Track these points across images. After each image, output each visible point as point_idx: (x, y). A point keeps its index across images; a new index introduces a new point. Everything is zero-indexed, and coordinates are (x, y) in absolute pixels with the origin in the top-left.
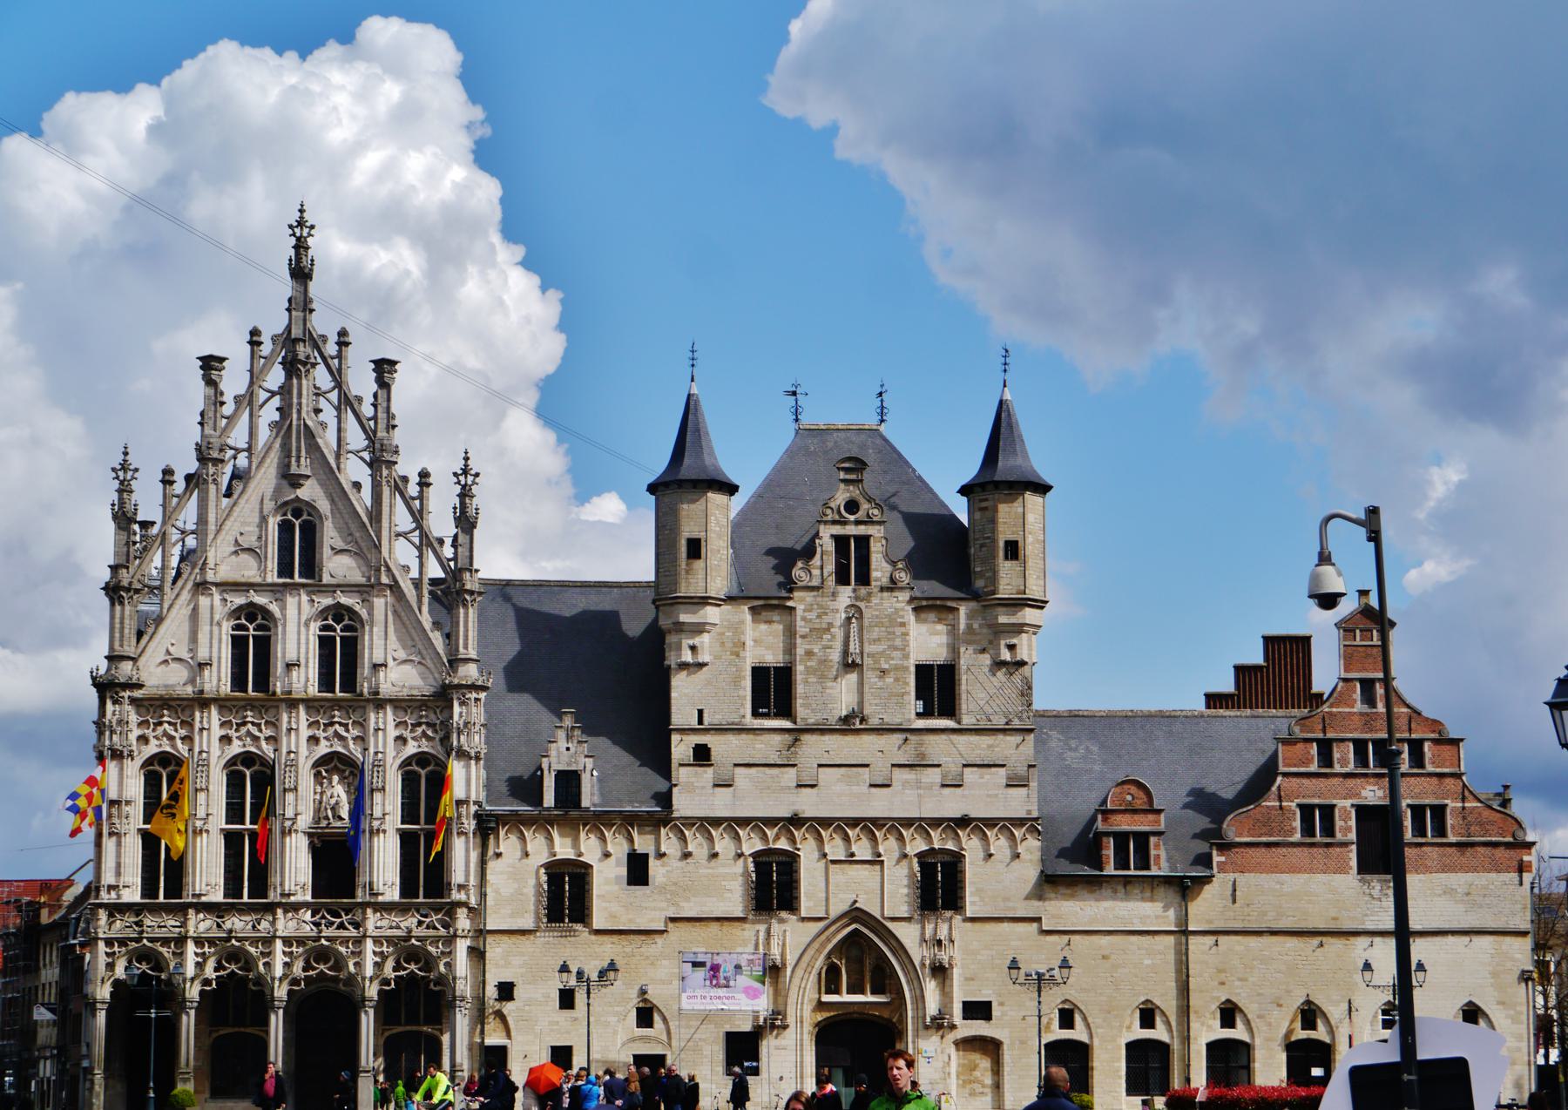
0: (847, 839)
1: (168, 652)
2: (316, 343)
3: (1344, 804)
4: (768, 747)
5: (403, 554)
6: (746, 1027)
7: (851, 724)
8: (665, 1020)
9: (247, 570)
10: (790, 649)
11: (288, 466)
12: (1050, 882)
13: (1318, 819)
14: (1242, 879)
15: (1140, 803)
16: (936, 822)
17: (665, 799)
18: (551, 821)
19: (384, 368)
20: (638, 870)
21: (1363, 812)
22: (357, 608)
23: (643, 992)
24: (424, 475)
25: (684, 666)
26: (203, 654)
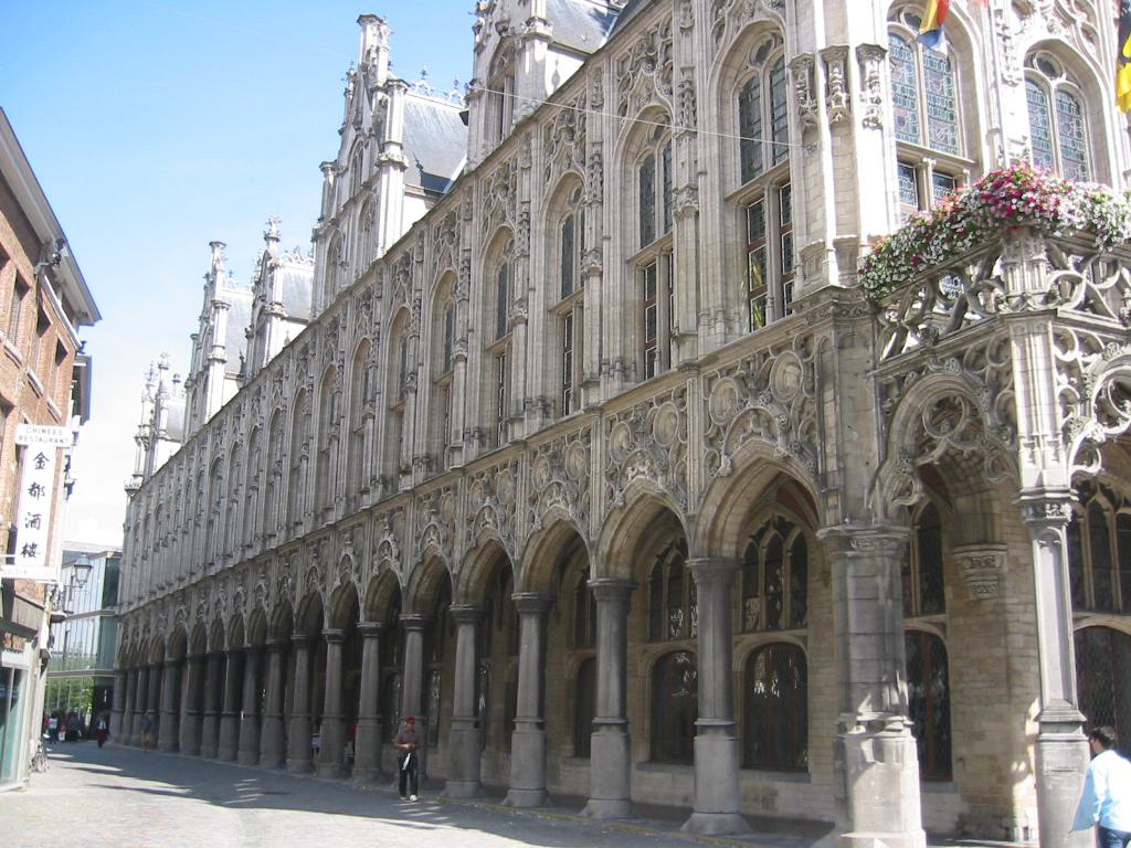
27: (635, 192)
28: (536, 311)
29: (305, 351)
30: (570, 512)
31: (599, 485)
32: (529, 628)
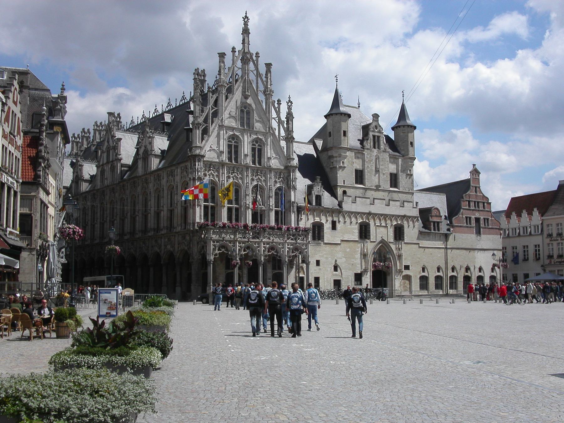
0: (380, 220)
1: (211, 147)
2: (251, 55)
3: (473, 217)
4: (359, 193)
5: (275, 124)
6: (359, 272)
7: (378, 188)
8: (340, 269)
9: (233, 124)
10: (363, 165)
11: (245, 92)
12: (421, 233)
13: (468, 219)
14: (457, 235)
15: (438, 214)
16: (399, 216)
17: (340, 205)
18: (314, 210)
19: (268, 66)
20: (334, 227)
21: (476, 218)
22: (263, 139)
23: (336, 261)
24: (279, 101)
25: (340, 167)
26: (221, 149)
27: (169, 197)
28: (152, 212)
29: (94, 194)
30: (158, 251)
31: (163, 247)
32: (152, 269)
